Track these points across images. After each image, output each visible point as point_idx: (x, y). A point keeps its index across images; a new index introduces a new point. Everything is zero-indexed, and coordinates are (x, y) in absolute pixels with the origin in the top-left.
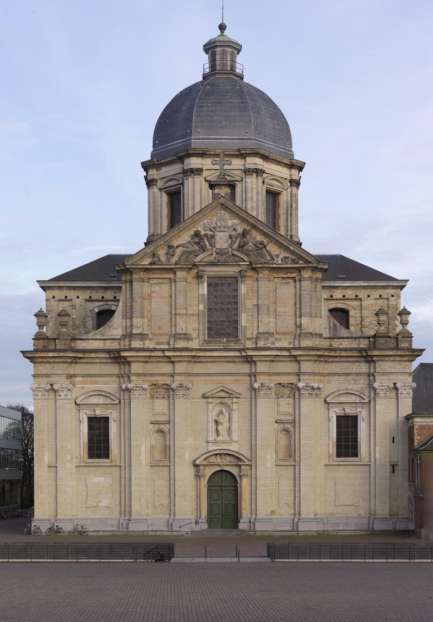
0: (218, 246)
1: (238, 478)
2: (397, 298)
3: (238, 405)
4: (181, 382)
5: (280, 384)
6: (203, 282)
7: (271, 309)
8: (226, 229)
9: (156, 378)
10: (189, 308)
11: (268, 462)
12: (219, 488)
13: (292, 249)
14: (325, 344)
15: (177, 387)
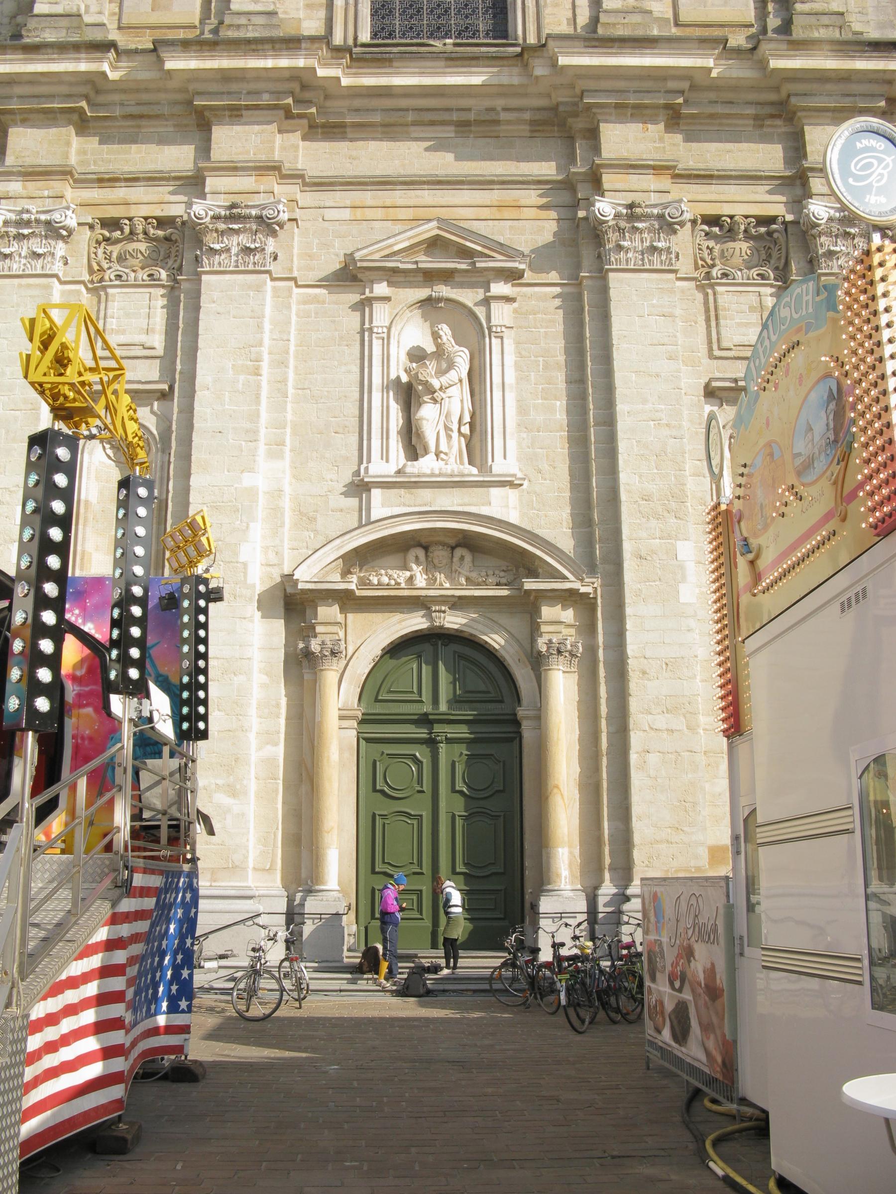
1: (522, 674)
3: (515, 311)
4: (237, 199)
5: (713, 220)
9: (121, 193)
11: (684, 579)
12: (422, 733)
15: (216, 218)
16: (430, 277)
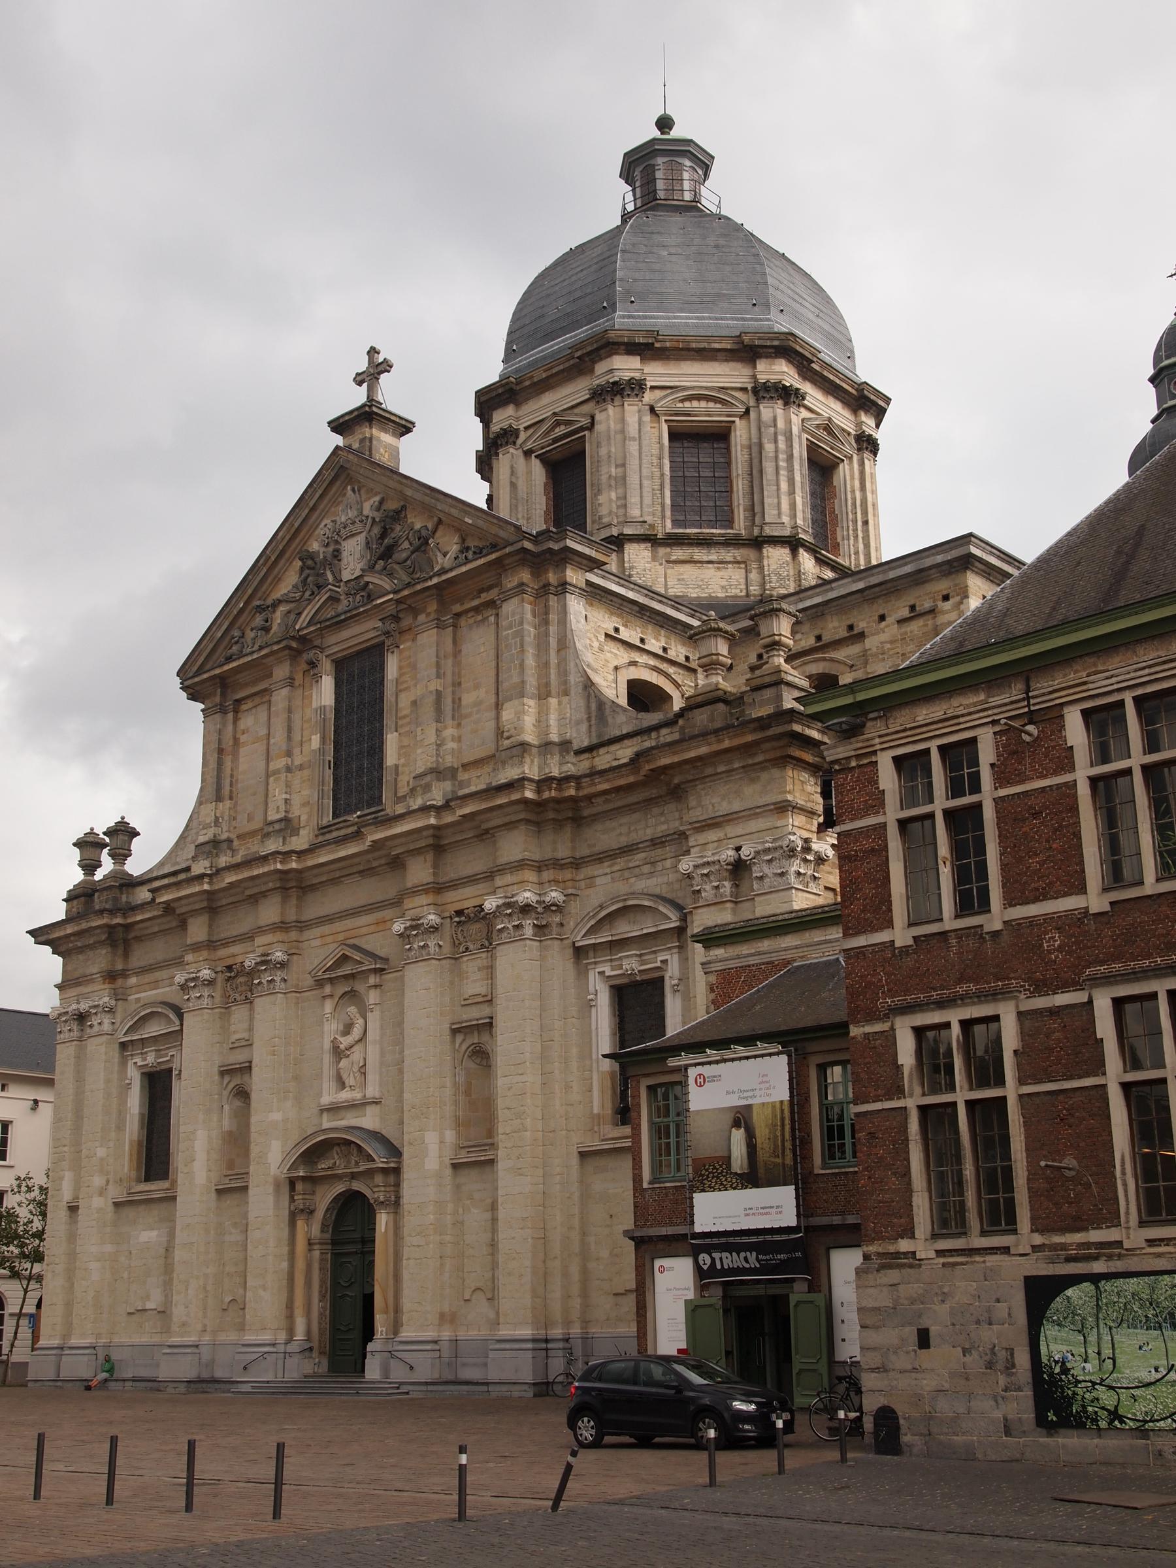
0: (346, 576)
2: (958, 599)
6: (317, 678)
7: (448, 701)
8: (358, 527)
10: (297, 751)
13: (470, 522)
14: (574, 766)
16: (346, 977)
